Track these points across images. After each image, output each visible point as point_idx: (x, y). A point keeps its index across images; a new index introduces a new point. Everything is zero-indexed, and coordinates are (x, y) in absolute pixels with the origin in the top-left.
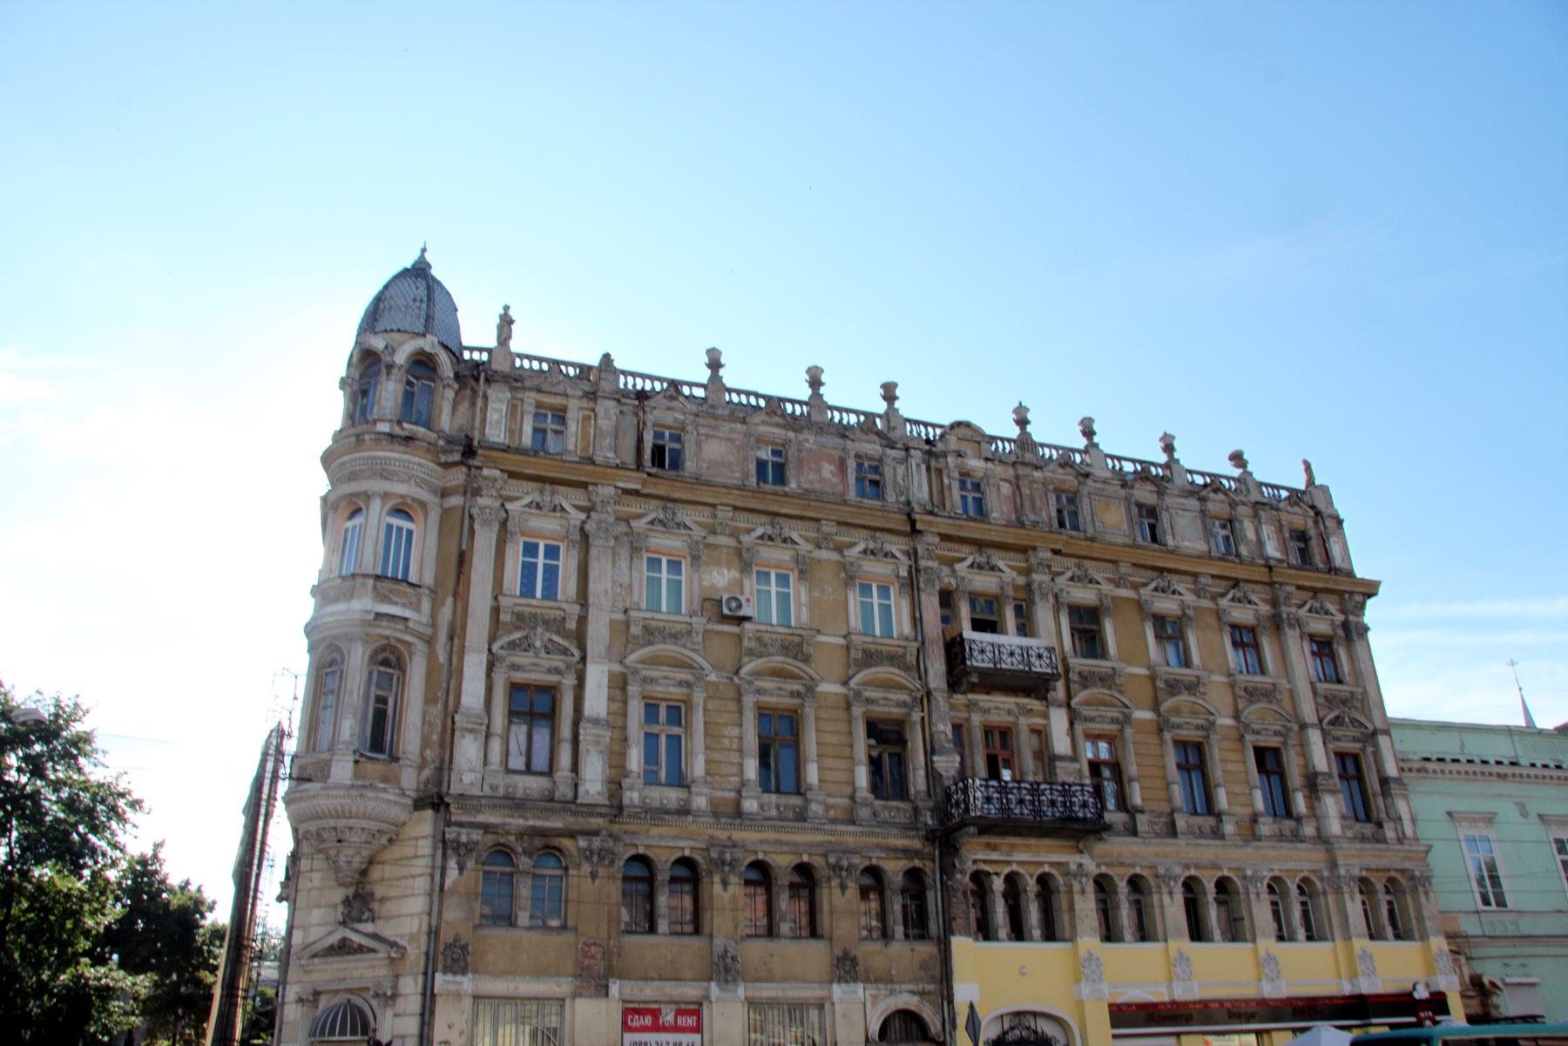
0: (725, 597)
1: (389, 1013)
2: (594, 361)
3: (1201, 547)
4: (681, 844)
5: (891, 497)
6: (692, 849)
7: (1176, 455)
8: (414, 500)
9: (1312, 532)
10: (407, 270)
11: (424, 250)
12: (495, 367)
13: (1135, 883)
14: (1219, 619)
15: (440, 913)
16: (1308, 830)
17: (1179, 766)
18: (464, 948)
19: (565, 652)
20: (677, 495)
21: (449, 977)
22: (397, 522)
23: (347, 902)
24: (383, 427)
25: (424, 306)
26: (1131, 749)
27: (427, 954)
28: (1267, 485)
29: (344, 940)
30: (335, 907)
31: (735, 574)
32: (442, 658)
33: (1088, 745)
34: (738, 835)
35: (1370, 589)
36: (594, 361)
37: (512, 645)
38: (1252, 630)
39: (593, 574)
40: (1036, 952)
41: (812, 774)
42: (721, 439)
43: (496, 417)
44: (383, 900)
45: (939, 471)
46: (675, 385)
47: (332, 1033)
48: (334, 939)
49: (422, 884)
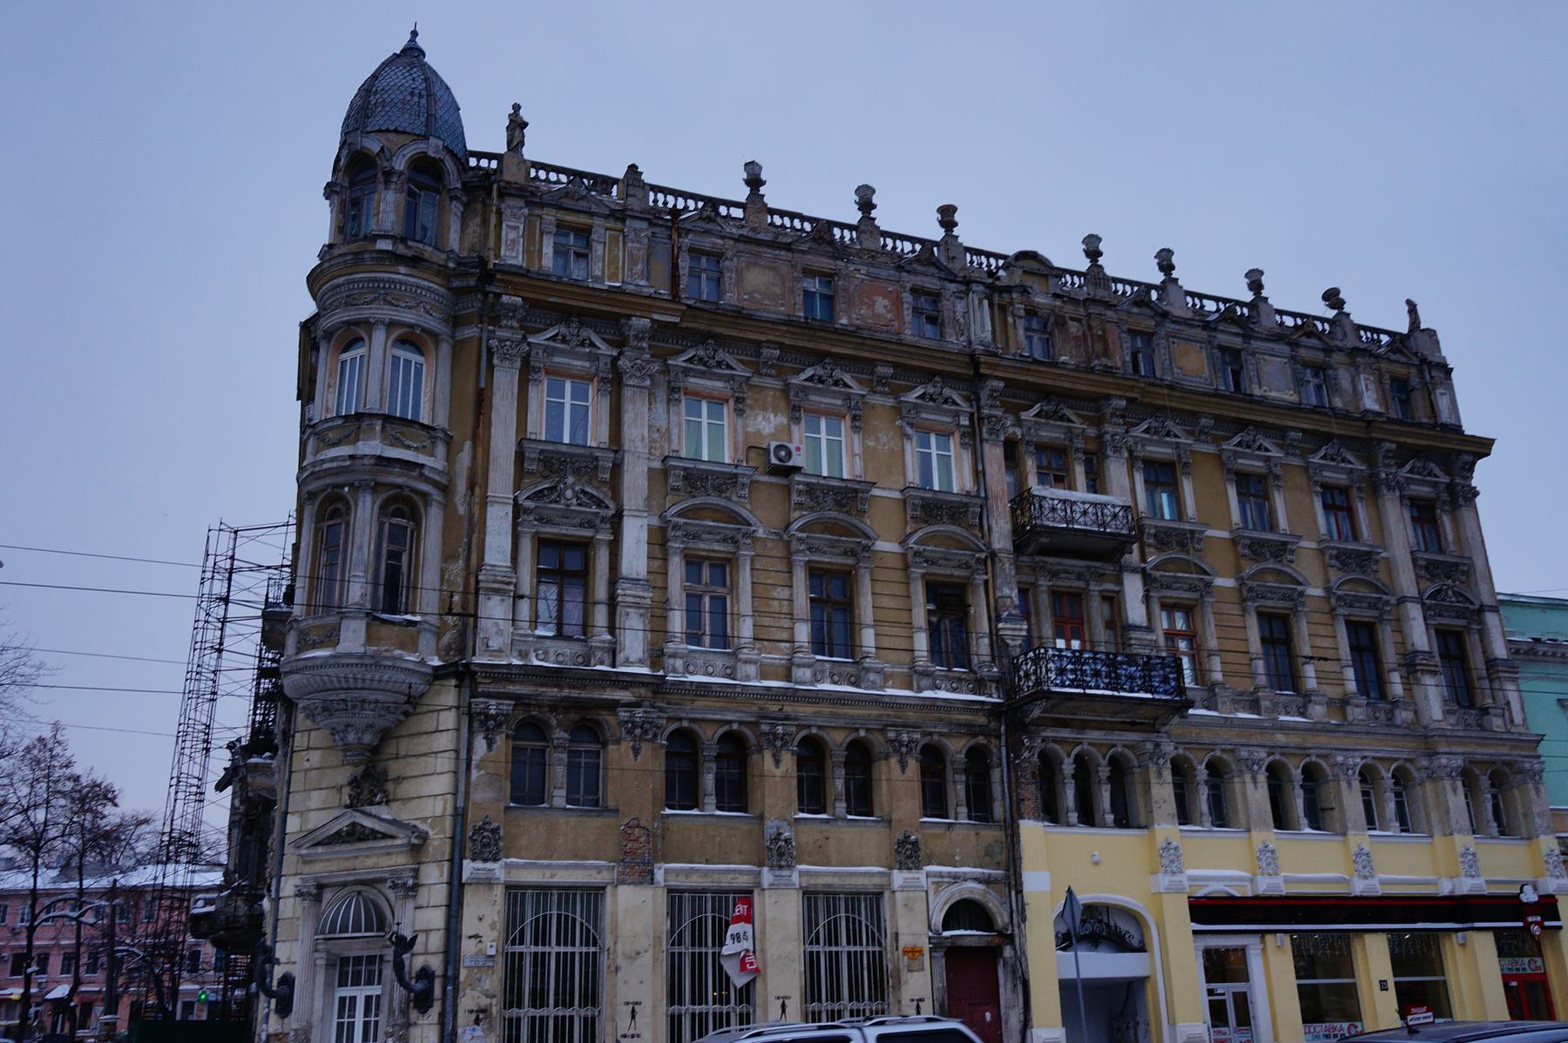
0: (773, 445)
1: (410, 905)
2: (619, 173)
3: (1290, 396)
4: (729, 717)
6: (740, 723)
7: (1264, 293)
8: (424, 330)
9: (1415, 381)
10: (396, 56)
11: (414, 34)
12: (507, 177)
13: (1215, 769)
14: (1309, 478)
15: (467, 793)
16: (1404, 715)
17: (1263, 640)
18: (495, 831)
19: (600, 503)
21: (479, 864)
22: (404, 354)
23: (354, 783)
24: (383, 245)
25: (423, 101)
26: (1210, 618)
27: (453, 838)
28: (1366, 329)
29: (354, 824)
30: (340, 789)
31: (782, 419)
32: (462, 510)
33: (1164, 615)
35: (1483, 447)
36: (619, 173)
37: (538, 496)
38: (1344, 491)
39: (628, 418)
40: (1108, 842)
41: (868, 638)
42: (765, 267)
43: (512, 235)
44: (399, 780)
45: (1003, 308)
46: (713, 203)
47: (344, 929)
48: (343, 824)
49: (445, 763)
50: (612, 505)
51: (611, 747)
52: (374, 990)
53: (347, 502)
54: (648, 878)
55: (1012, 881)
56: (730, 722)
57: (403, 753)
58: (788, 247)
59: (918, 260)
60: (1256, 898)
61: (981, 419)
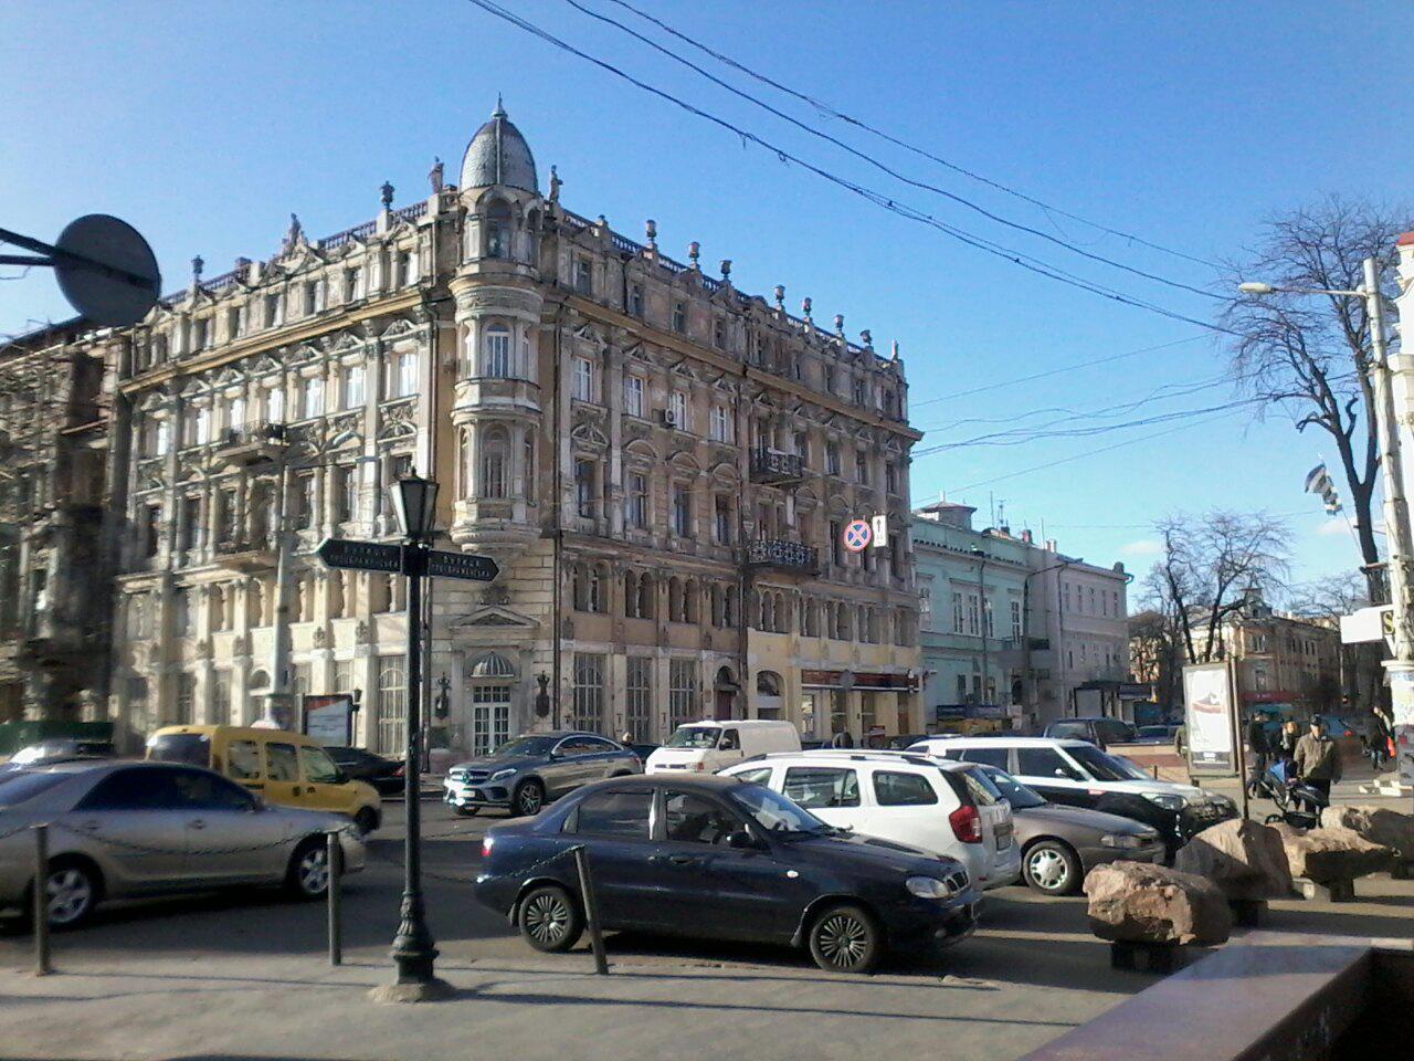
5: (729, 348)
19: (601, 440)
20: (649, 339)
34: (670, 562)
35: (918, 436)
37: (578, 434)
41: (696, 527)
49: (549, 585)
50: (607, 441)
51: (609, 580)
52: (502, 705)
53: (506, 431)
54: (623, 651)
55: (742, 659)
56: (645, 568)
57: (518, 577)
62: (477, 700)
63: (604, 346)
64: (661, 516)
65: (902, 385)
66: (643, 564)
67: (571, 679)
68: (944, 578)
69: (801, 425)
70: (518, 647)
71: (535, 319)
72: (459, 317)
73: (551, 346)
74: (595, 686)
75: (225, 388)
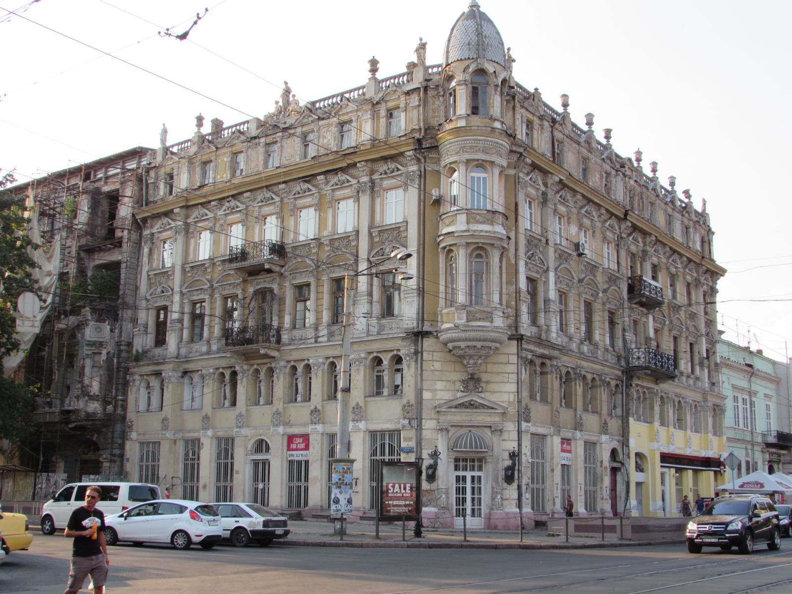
9: (706, 239)
30: (454, 382)
32: (513, 261)
41: (597, 337)
44: (487, 382)
49: (514, 377)
52: (476, 473)
54: (558, 432)
58: (579, 143)
59: (607, 157)
60: (668, 454)
61: (621, 238)
62: (457, 468)
63: (543, 188)
64: (576, 328)
65: (710, 232)
66: (567, 361)
67: (529, 454)
68: (729, 383)
69: (655, 260)
70: (490, 427)
71: (505, 164)
72: (447, 160)
73: (512, 185)
74: (540, 461)
75: (226, 215)
